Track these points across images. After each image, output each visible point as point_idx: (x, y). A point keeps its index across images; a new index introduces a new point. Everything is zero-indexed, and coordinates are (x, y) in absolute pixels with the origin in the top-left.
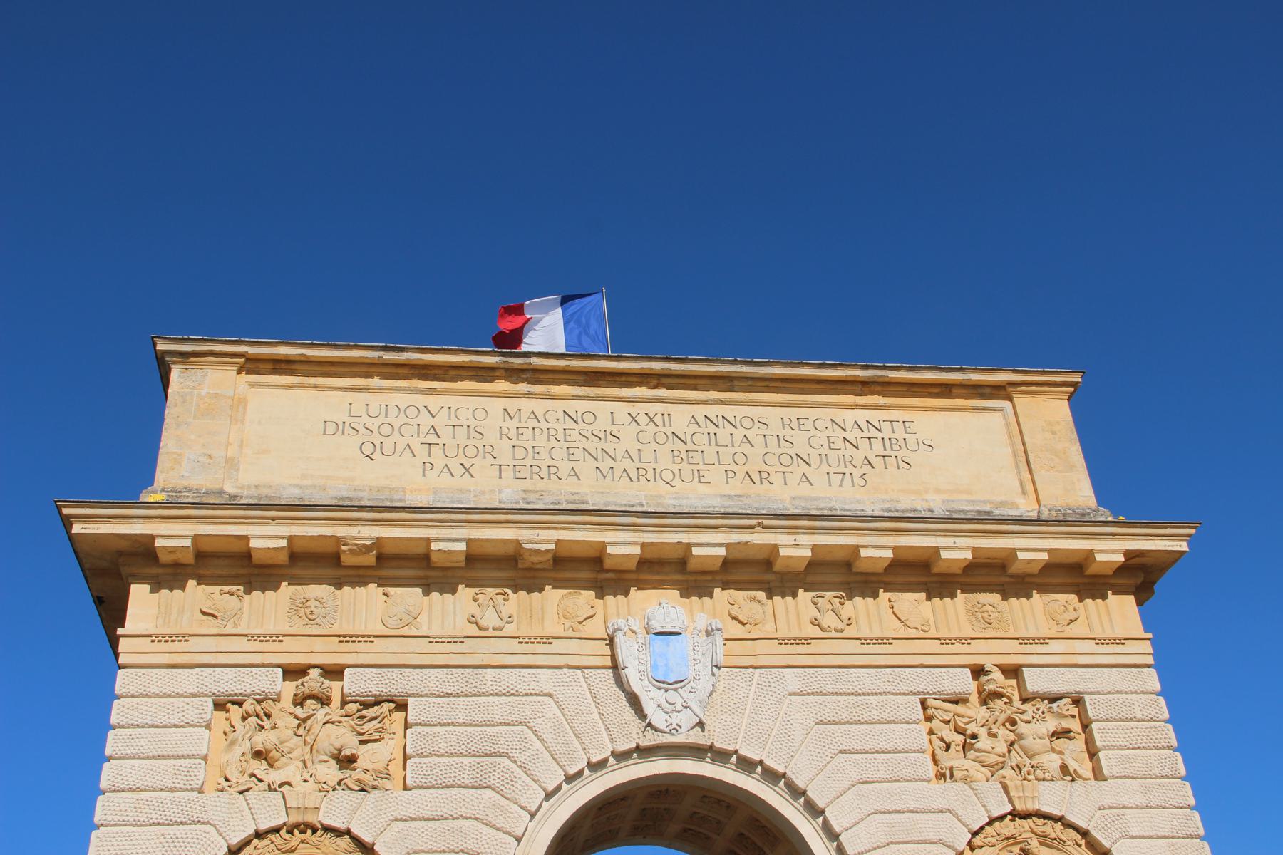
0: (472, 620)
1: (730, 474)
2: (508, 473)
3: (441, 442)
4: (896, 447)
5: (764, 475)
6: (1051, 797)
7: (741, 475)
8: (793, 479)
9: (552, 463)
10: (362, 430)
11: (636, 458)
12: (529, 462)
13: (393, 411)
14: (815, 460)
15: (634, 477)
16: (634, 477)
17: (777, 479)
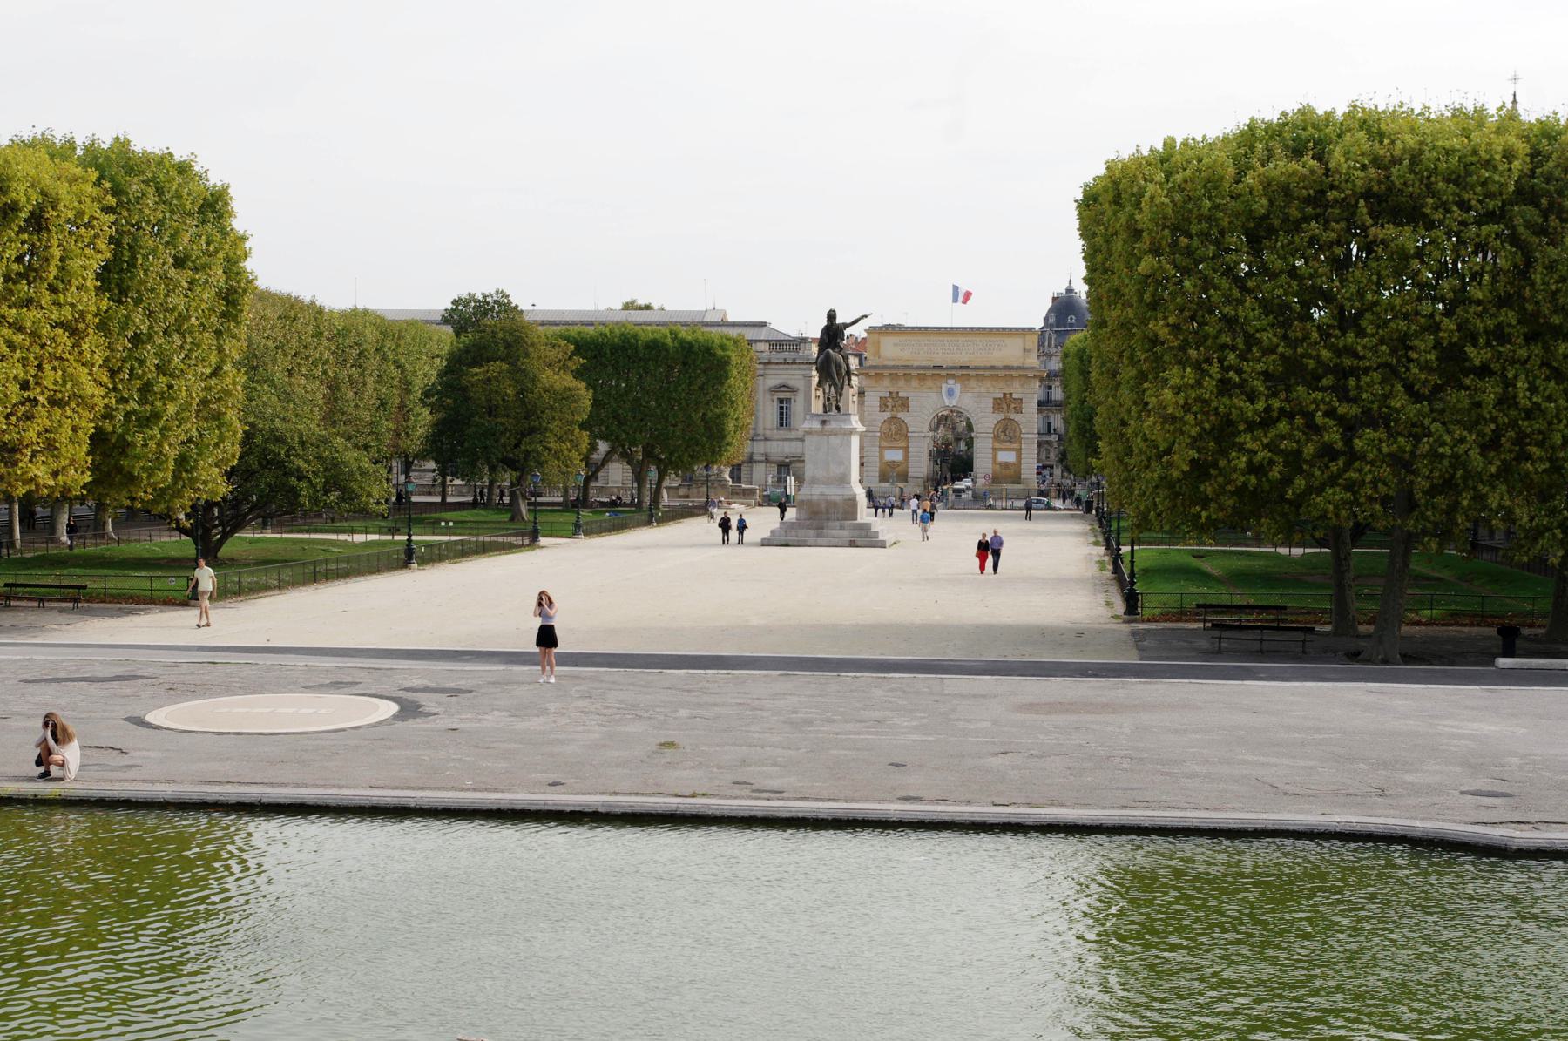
6: (1013, 416)
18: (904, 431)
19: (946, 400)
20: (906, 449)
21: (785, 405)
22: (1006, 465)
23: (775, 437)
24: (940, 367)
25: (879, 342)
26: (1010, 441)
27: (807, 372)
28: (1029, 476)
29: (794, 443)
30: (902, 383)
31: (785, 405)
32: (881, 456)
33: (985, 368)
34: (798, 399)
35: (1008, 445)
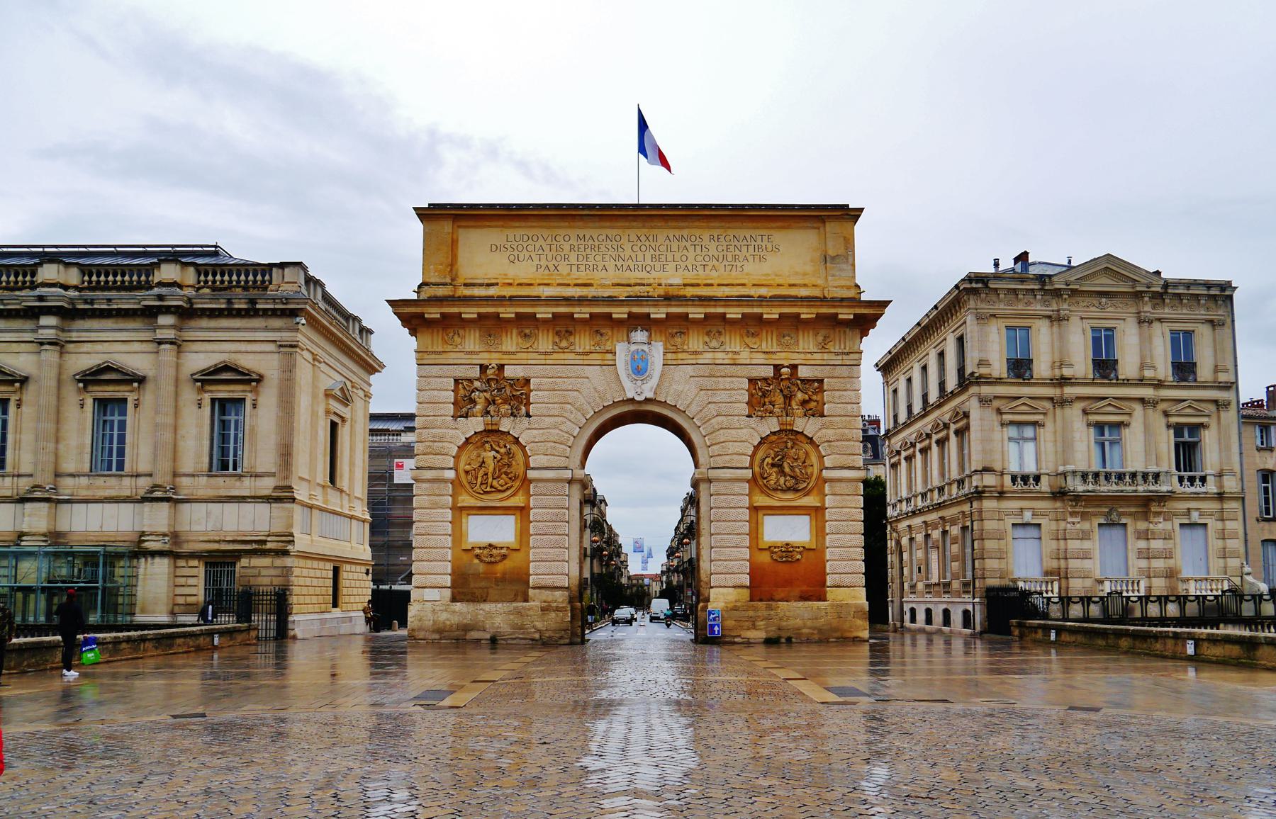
0: (555, 343)
1: (678, 267)
2: (574, 268)
3: (545, 253)
4: (760, 250)
5: (694, 267)
6: (800, 424)
7: (683, 267)
8: (708, 268)
9: (595, 263)
10: (509, 249)
11: (634, 260)
12: (584, 262)
13: (526, 238)
14: (721, 260)
15: (633, 270)
16: (633, 270)
17: (700, 269)
18: (518, 467)
19: (627, 384)
20: (523, 511)
21: (232, 418)
22: (786, 552)
23: (201, 493)
24: (611, 300)
25: (454, 244)
26: (797, 491)
27: (286, 336)
28: (847, 579)
29: (248, 508)
30: (510, 342)
31: (232, 418)
32: (458, 534)
33: (728, 301)
34: (261, 400)
35: (788, 499)
